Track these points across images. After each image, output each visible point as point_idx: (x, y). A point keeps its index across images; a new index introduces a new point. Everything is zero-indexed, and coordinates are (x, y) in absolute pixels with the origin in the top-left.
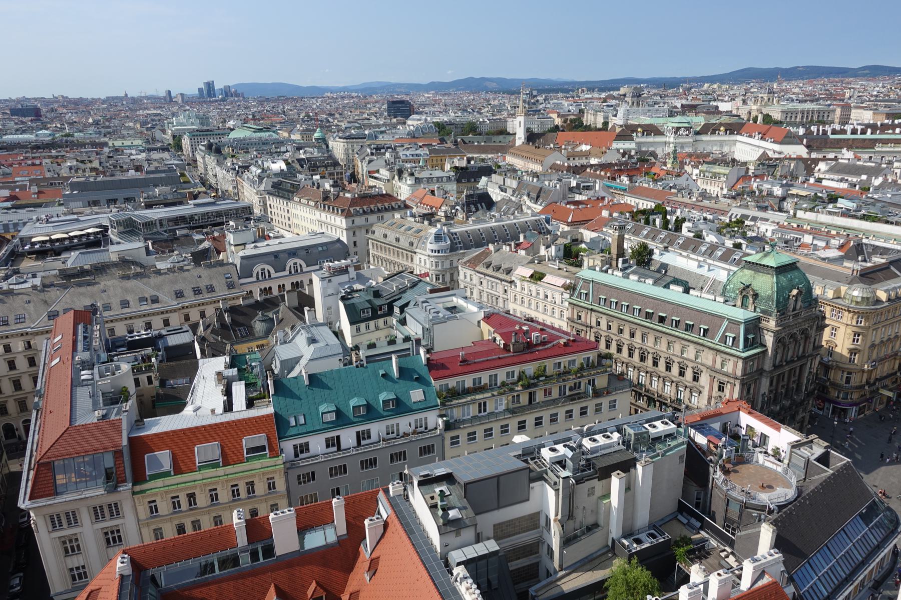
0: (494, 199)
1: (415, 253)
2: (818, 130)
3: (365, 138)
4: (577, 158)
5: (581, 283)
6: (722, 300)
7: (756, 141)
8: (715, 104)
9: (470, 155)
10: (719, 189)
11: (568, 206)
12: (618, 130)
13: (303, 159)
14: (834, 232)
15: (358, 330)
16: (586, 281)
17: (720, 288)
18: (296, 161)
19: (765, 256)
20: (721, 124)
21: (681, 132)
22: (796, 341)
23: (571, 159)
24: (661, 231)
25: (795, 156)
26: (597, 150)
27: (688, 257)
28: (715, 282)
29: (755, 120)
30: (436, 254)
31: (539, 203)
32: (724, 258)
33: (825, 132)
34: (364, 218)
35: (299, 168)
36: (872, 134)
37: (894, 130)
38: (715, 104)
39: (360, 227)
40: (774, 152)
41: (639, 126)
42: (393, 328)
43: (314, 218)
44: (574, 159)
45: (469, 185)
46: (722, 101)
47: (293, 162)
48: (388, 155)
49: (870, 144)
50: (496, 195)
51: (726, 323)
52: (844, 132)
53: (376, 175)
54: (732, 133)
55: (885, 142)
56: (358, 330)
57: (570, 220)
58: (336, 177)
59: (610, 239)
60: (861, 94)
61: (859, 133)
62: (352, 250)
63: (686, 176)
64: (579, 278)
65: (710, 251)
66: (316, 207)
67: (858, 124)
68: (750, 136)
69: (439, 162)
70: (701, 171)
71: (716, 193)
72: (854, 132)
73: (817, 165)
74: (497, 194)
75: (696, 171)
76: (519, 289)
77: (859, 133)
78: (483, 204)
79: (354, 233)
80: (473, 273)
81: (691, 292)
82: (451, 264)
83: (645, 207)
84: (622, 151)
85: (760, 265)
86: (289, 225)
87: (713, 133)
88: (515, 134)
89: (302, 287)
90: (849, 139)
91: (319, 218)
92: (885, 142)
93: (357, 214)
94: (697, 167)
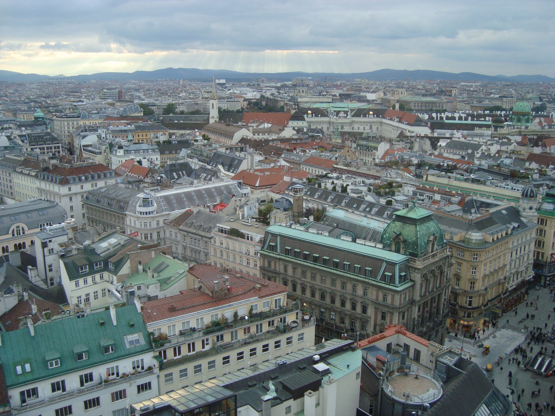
0: (193, 167)
1: (126, 215)
2: (437, 117)
3: (79, 117)
4: (261, 134)
5: (270, 236)
6: (380, 246)
7: (395, 124)
8: (364, 94)
9: (172, 131)
10: (372, 160)
11: (256, 173)
12: (293, 112)
13: (24, 136)
14: (454, 192)
15: (77, 284)
16: (274, 235)
17: (379, 237)
18: (18, 137)
19: (410, 211)
20: (370, 110)
21: (342, 114)
22: (434, 276)
23: (256, 135)
24: (331, 193)
25: (423, 135)
26: (277, 128)
27: (353, 212)
28: (375, 232)
29: (394, 107)
30: (145, 216)
31: (231, 171)
32: (380, 214)
33: (441, 118)
34: (79, 186)
35: (21, 143)
36: (472, 120)
37: (485, 119)
38: (364, 94)
39: (76, 194)
40: (409, 131)
41: (309, 109)
42: (108, 282)
43: (34, 186)
44: (258, 134)
45: (171, 156)
46: (368, 92)
47: (15, 137)
48: (100, 131)
49: (471, 127)
50: (195, 164)
51: (384, 265)
52: (454, 118)
53: (90, 148)
54: (378, 116)
55: (481, 126)
56: (77, 284)
57: (257, 185)
58: (53, 150)
59: (292, 200)
60: (462, 92)
61: (463, 119)
62: (69, 213)
63: (347, 149)
64: (269, 233)
65: (368, 209)
66: (36, 176)
67: (463, 113)
68: (391, 119)
69: (144, 137)
70: (358, 145)
71: (370, 162)
72: (460, 118)
73: (438, 142)
74: (195, 164)
75: (354, 145)
76: (218, 244)
77: (463, 119)
78: (184, 172)
79: (71, 199)
80: (177, 231)
81: (358, 241)
82: (158, 223)
83: (317, 173)
84: (296, 128)
85: (407, 217)
86: (12, 193)
87: (365, 116)
88: (209, 114)
89: (24, 247)
90: (457, 124)
91: (39, 186)
92: (481, 126)
93: (74, 182)
94: (355, 142)
